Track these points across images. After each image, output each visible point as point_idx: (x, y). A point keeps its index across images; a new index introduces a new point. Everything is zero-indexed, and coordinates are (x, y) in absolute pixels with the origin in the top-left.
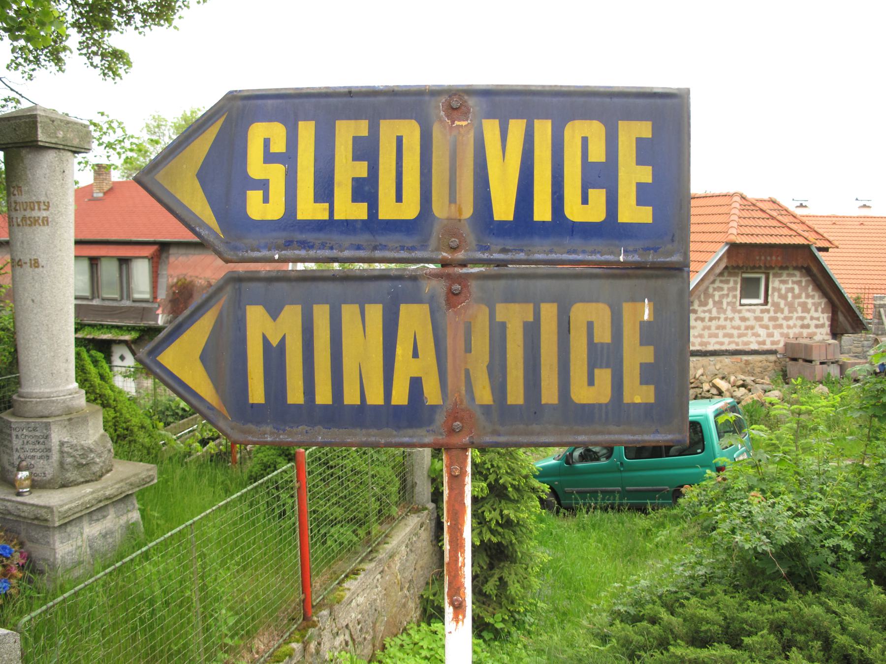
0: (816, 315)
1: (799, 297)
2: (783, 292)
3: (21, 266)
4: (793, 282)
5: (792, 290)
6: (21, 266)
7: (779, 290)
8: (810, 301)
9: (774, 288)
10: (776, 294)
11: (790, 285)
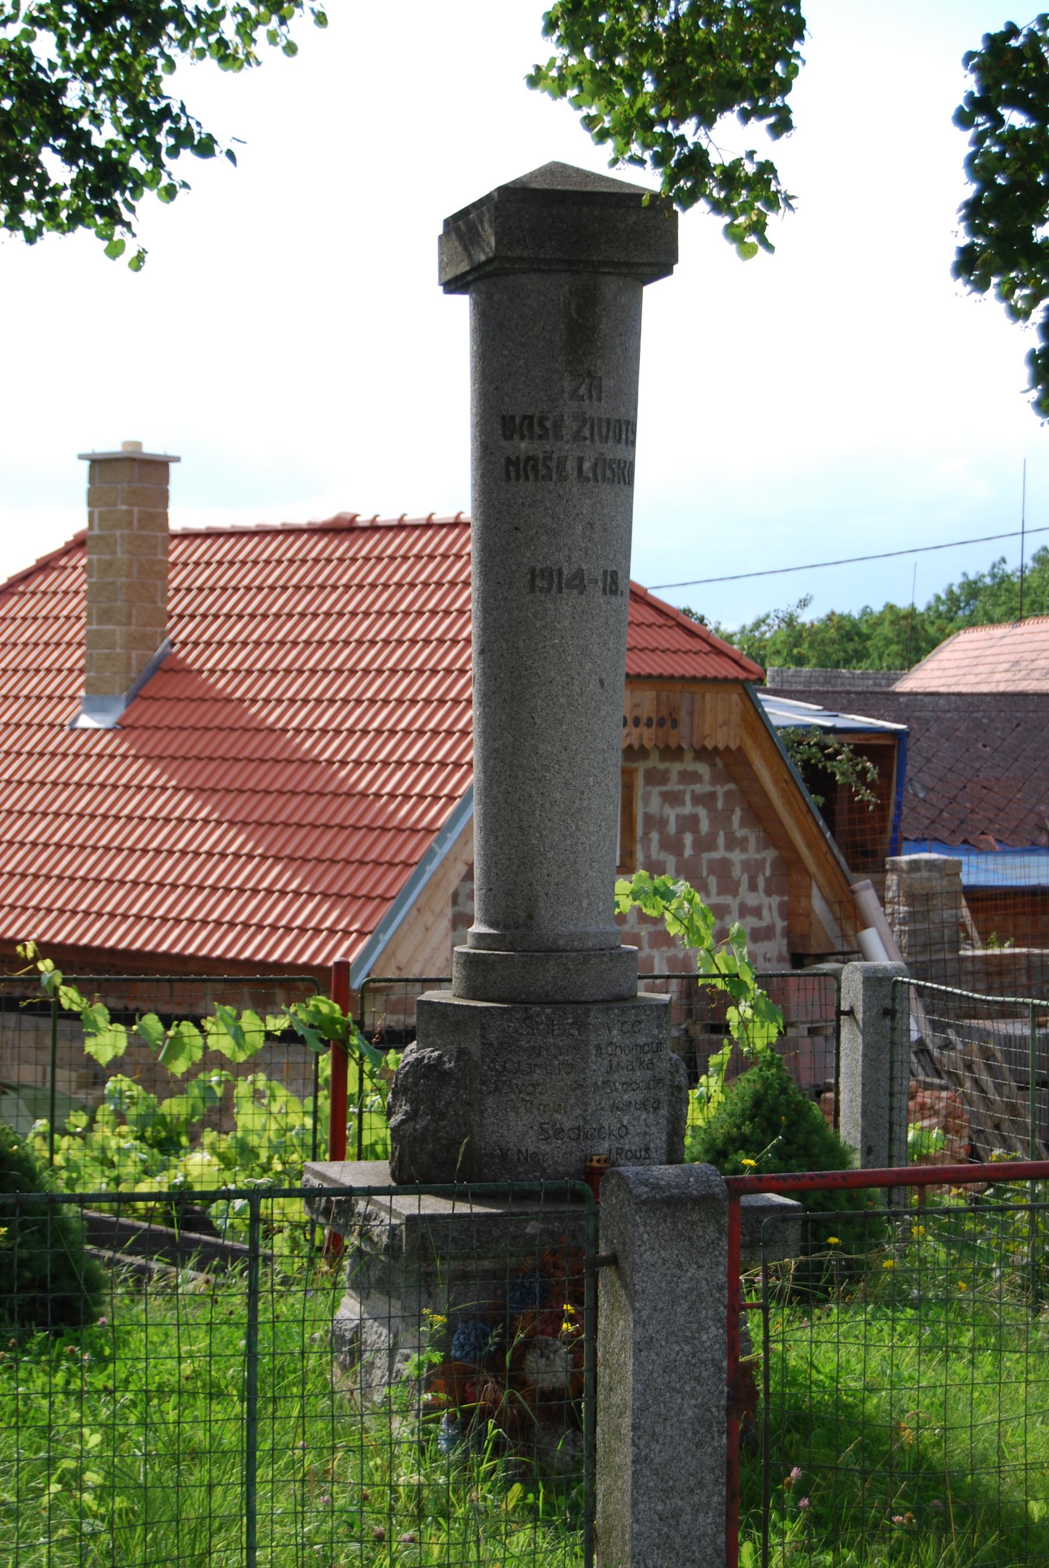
0: (752, 900)
1: (712, 846)
2: (672, 828)
3: (582, 589)
4: (697, 800)
5: (694, 819)
6: (582, 589)
7: (663, 822)
8: (736, 857)
9: (648, 818)
10: (655, 836)
11: (688, 809)
